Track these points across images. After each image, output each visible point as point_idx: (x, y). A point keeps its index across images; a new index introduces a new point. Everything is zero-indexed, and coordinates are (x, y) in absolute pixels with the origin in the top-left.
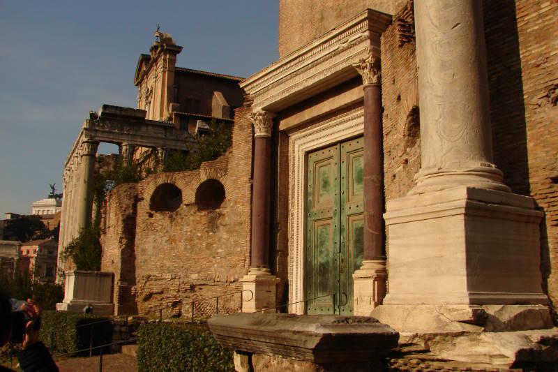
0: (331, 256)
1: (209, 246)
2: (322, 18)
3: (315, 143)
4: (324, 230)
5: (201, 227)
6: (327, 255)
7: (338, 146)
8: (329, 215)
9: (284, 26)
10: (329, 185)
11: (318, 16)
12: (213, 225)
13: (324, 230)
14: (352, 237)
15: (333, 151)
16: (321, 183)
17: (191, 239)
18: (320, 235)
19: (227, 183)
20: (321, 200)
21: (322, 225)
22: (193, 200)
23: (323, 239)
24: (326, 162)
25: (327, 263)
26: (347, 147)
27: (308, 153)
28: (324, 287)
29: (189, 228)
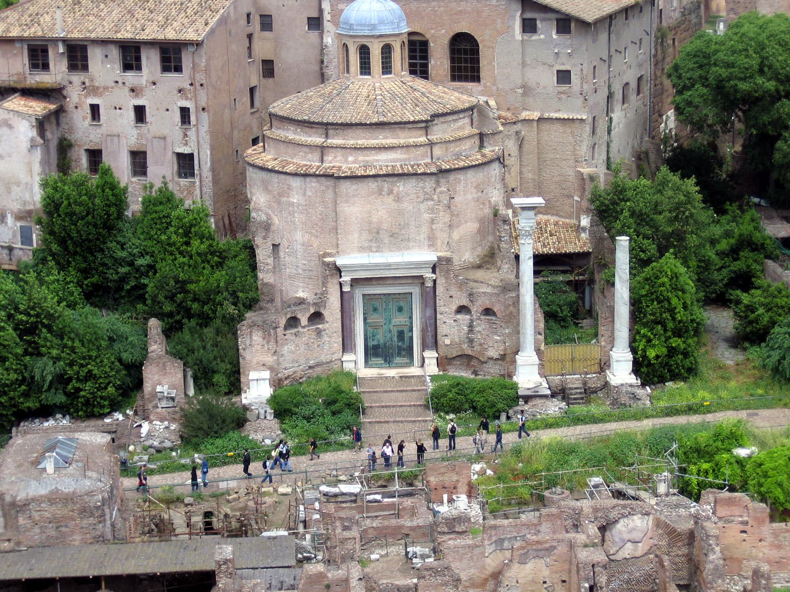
0: (382, 341)
1: (318, 346)
2: (378, 233)
5: (313, 336)
9: (342, 224)
11: (375, 230)
12: (319, 333)
14: (396, 334)
15: (381, 296)
16: (372, 309)
17: (308, 344)
19: (326, 313)
22: (306, 323)
27: (364, 295)
28: (377, 355)
29: (306, 338)
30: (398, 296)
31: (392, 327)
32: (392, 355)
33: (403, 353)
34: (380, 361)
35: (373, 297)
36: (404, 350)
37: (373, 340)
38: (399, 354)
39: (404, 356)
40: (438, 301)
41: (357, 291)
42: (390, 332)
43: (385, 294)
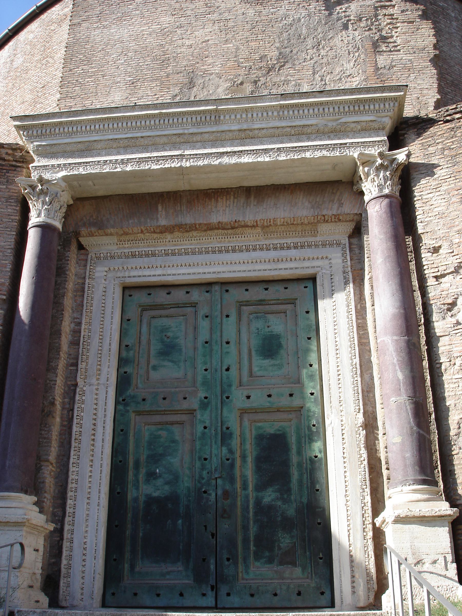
0: (186, 483)
3: (159, 272)
4: (164, 433)
6: (175, 479)
7: (217, 288)
8: (185, 405)
10: (181, 350)
11: (182, 78)
13: (164, 433)
15: (195, 295)
16: (155, 347)
18: (150, 443)
20: (154, 375)
21: (160, 423)
23: (161, 450)
24: (172, 311)
25: (173, 498)
26: (237, 294)
28: (160, 549)
30: (256, 293)
31: (232, 420)
32: (232, 543)
33: (285, 541)
34: (176, 574)
35: (161, 297)
36: (288, 524)
37: (151, 476)
38: (265, 547)
39: (288, 559)
40: (425, 255)
41: (100, 271)
42: (226, 436)
43: (207, 286)
